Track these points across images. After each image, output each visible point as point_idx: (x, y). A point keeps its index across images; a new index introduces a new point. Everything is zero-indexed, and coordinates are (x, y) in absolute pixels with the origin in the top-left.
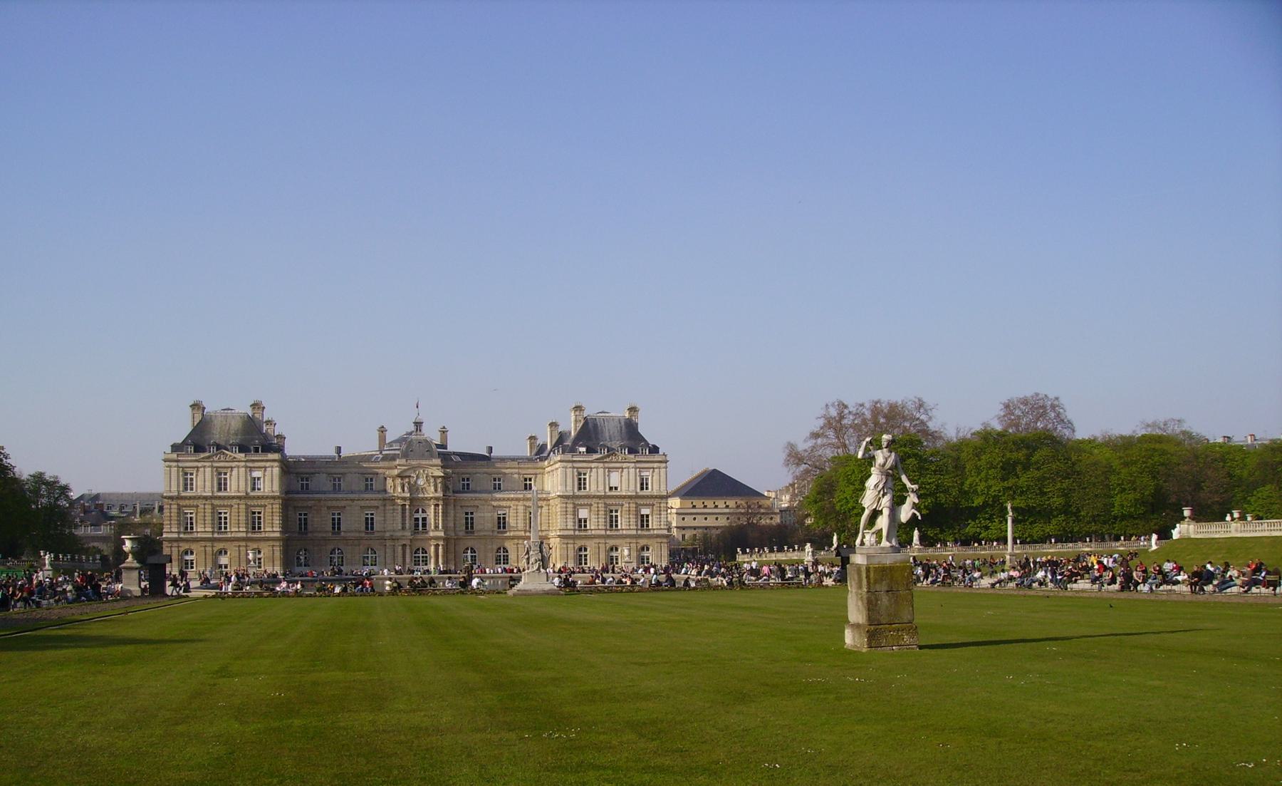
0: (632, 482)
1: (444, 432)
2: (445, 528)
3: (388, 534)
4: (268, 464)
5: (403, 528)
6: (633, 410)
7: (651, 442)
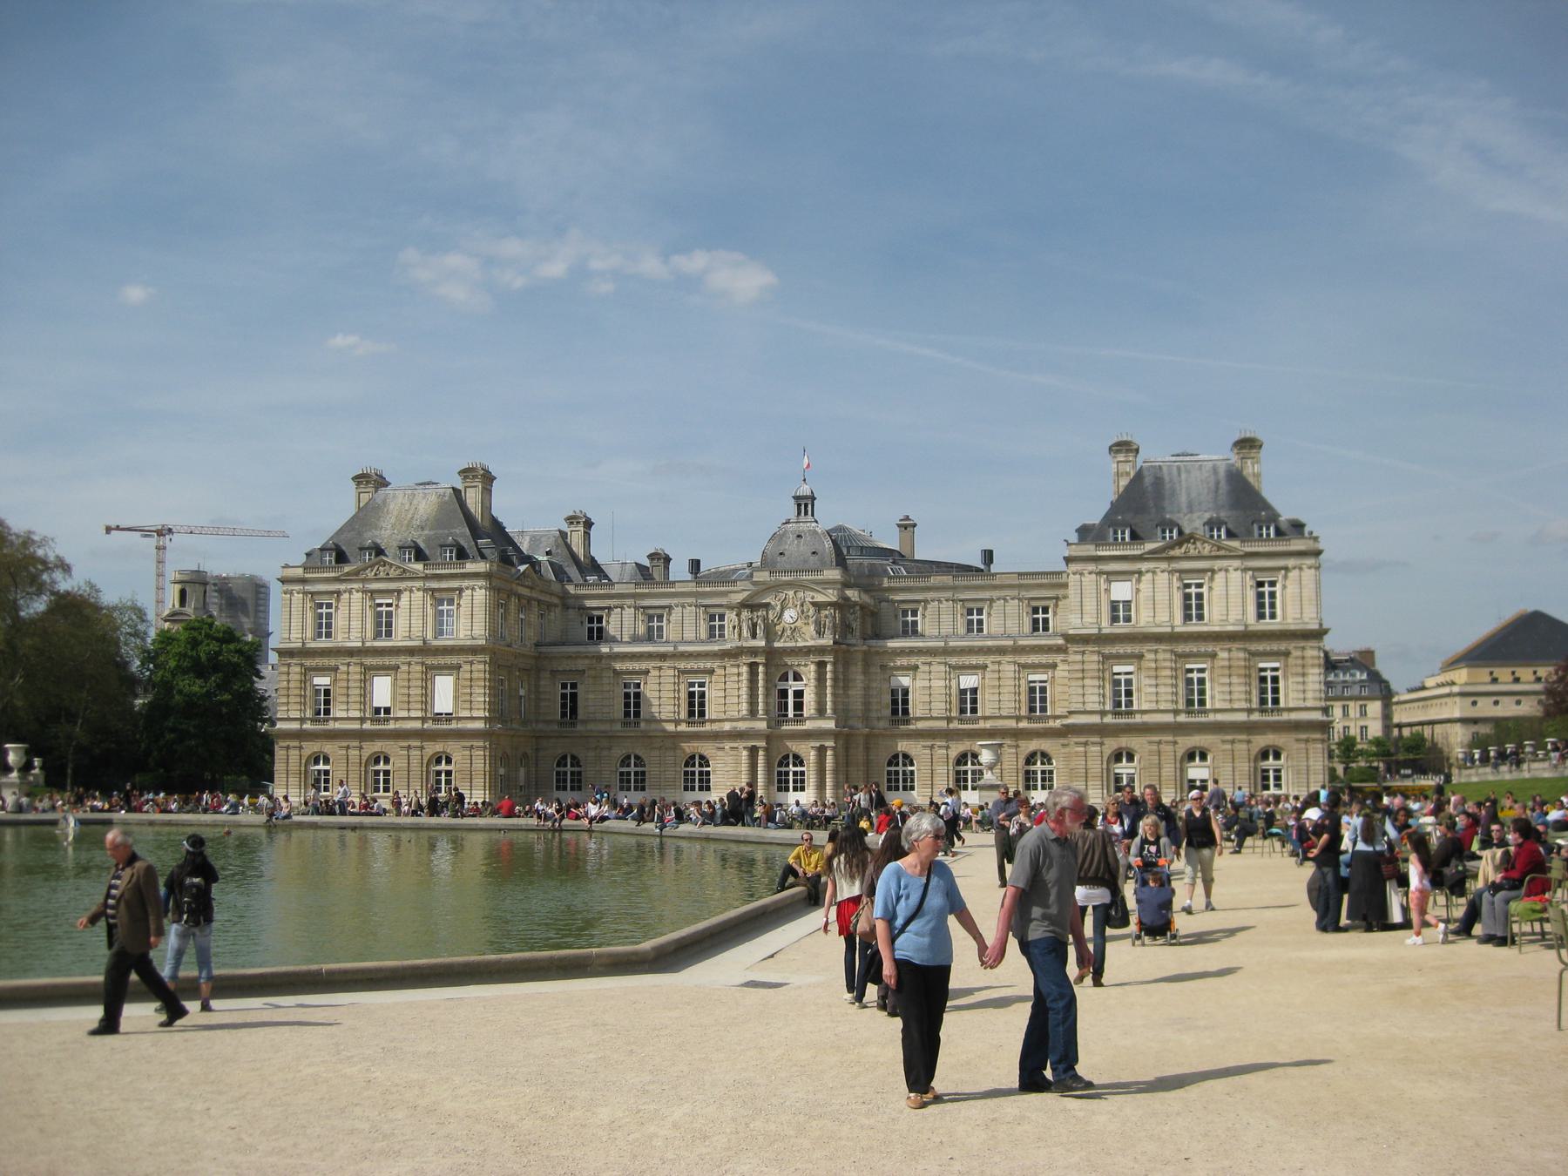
0: (1235, 600)
1: (907, 526)
2: (842, 714)
3: (727, 726)
4: (465, 583)
5: (753, 713)
6: (1247, 445)
7: (1286, 514)
